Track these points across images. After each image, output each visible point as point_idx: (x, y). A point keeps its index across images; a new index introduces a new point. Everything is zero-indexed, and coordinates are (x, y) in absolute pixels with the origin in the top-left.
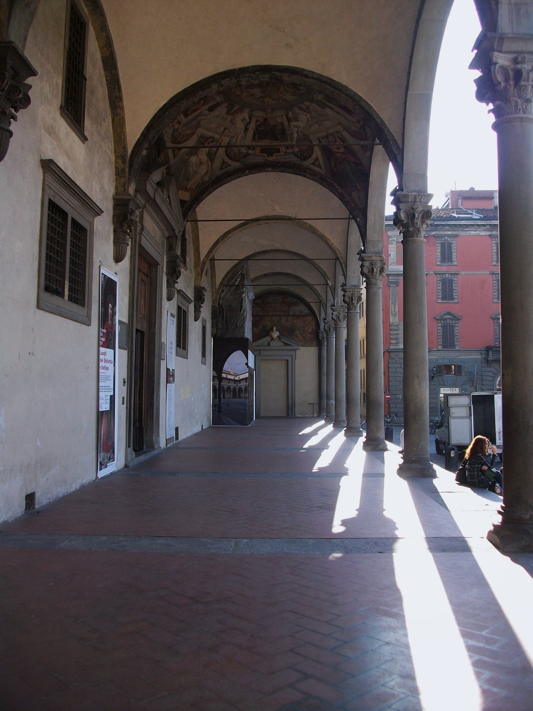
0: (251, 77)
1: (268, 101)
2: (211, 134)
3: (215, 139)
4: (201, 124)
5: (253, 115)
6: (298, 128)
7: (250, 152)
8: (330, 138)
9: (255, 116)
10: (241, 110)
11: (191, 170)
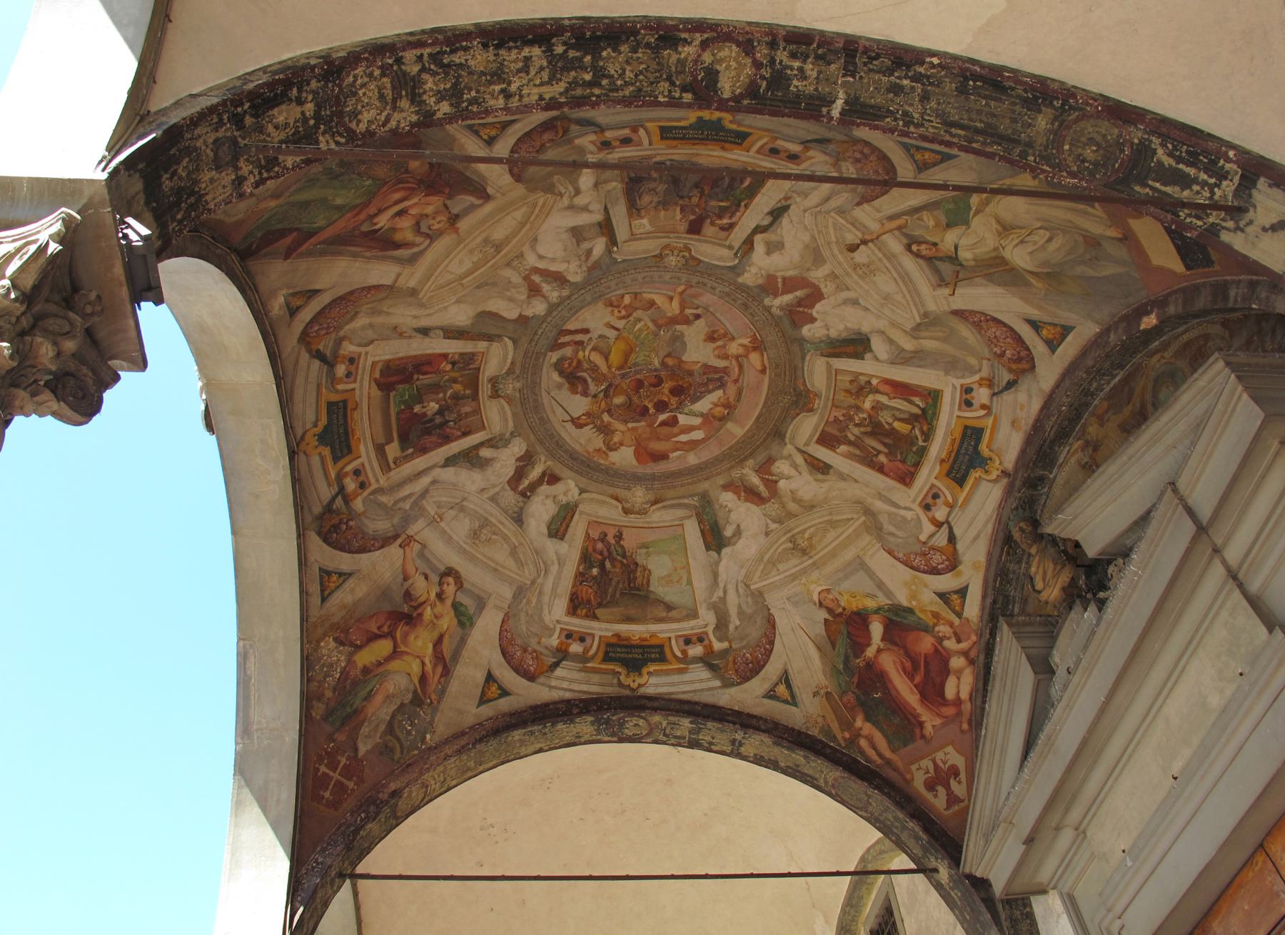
0: (665, 735)
1: (671, 298)
2: (909, 263)
3: (905, 241)
4: (918, 320)
5: (736, 254)
6: (571, 207)
7: (795, 148)
8: (439, 223)
9: (730, 247)
10: (770, 286)
11: (1053, 246)
